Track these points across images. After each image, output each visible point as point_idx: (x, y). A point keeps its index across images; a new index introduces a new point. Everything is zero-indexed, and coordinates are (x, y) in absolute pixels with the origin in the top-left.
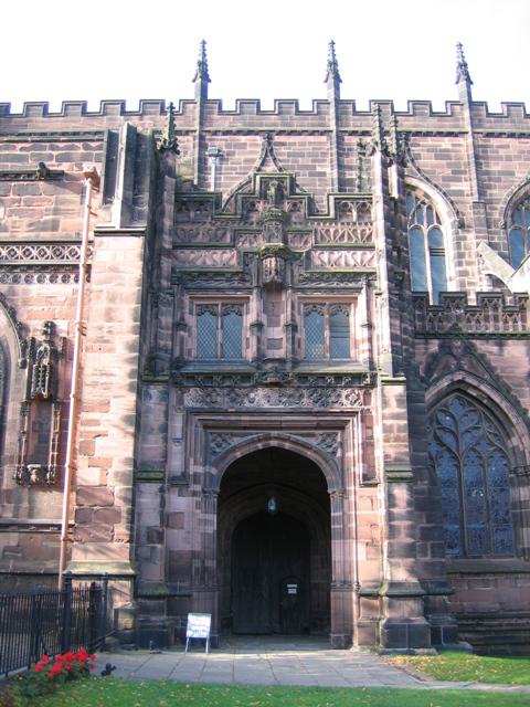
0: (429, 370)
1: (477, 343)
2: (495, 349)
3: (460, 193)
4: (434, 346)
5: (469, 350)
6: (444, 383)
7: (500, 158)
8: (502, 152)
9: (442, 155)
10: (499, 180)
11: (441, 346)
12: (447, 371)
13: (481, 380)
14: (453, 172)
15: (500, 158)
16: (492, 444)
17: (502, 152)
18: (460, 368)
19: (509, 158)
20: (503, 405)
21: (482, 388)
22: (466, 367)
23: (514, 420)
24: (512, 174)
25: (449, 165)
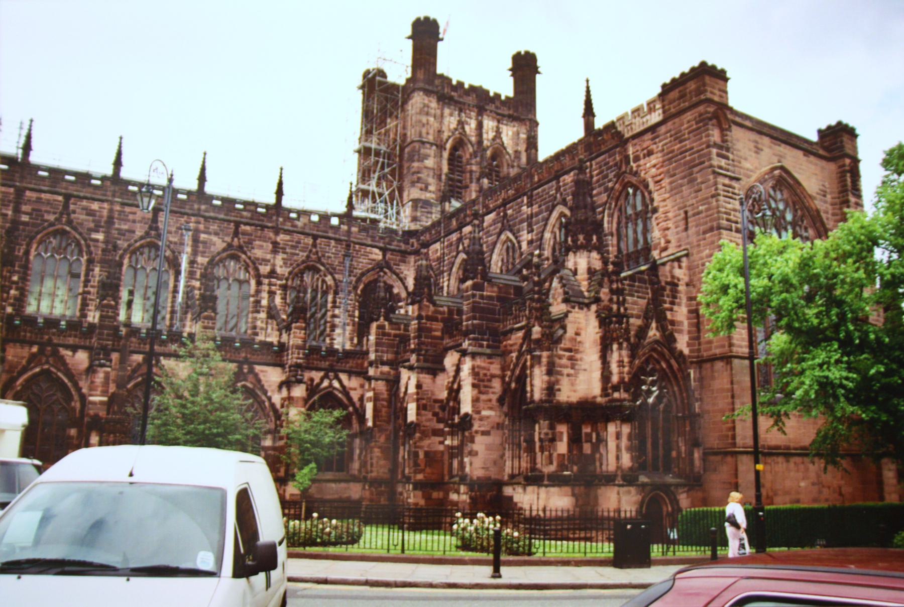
0: (29, 361)
1: (61, 349)
2: (70, 353)
3: (97, 241)
4: (35, 349)
5: (56, 354)
6: (37, 370)
7: (129, 221)
8: (131, 217)
9: (91, 213)
10: (124, 235)
11: (39, 350)
12: (39, 364)
13: (59, 370)
14: (96, 226)
15: (129, 221)
16: (61, 404)
17: (131, 217)
18: (47, 362)
19: (134, 221)
20: (69, 384)
21: (60, 374)
22: (51, 362)
23: (74, 393)
24: (134, 232)
25: (94, 221)
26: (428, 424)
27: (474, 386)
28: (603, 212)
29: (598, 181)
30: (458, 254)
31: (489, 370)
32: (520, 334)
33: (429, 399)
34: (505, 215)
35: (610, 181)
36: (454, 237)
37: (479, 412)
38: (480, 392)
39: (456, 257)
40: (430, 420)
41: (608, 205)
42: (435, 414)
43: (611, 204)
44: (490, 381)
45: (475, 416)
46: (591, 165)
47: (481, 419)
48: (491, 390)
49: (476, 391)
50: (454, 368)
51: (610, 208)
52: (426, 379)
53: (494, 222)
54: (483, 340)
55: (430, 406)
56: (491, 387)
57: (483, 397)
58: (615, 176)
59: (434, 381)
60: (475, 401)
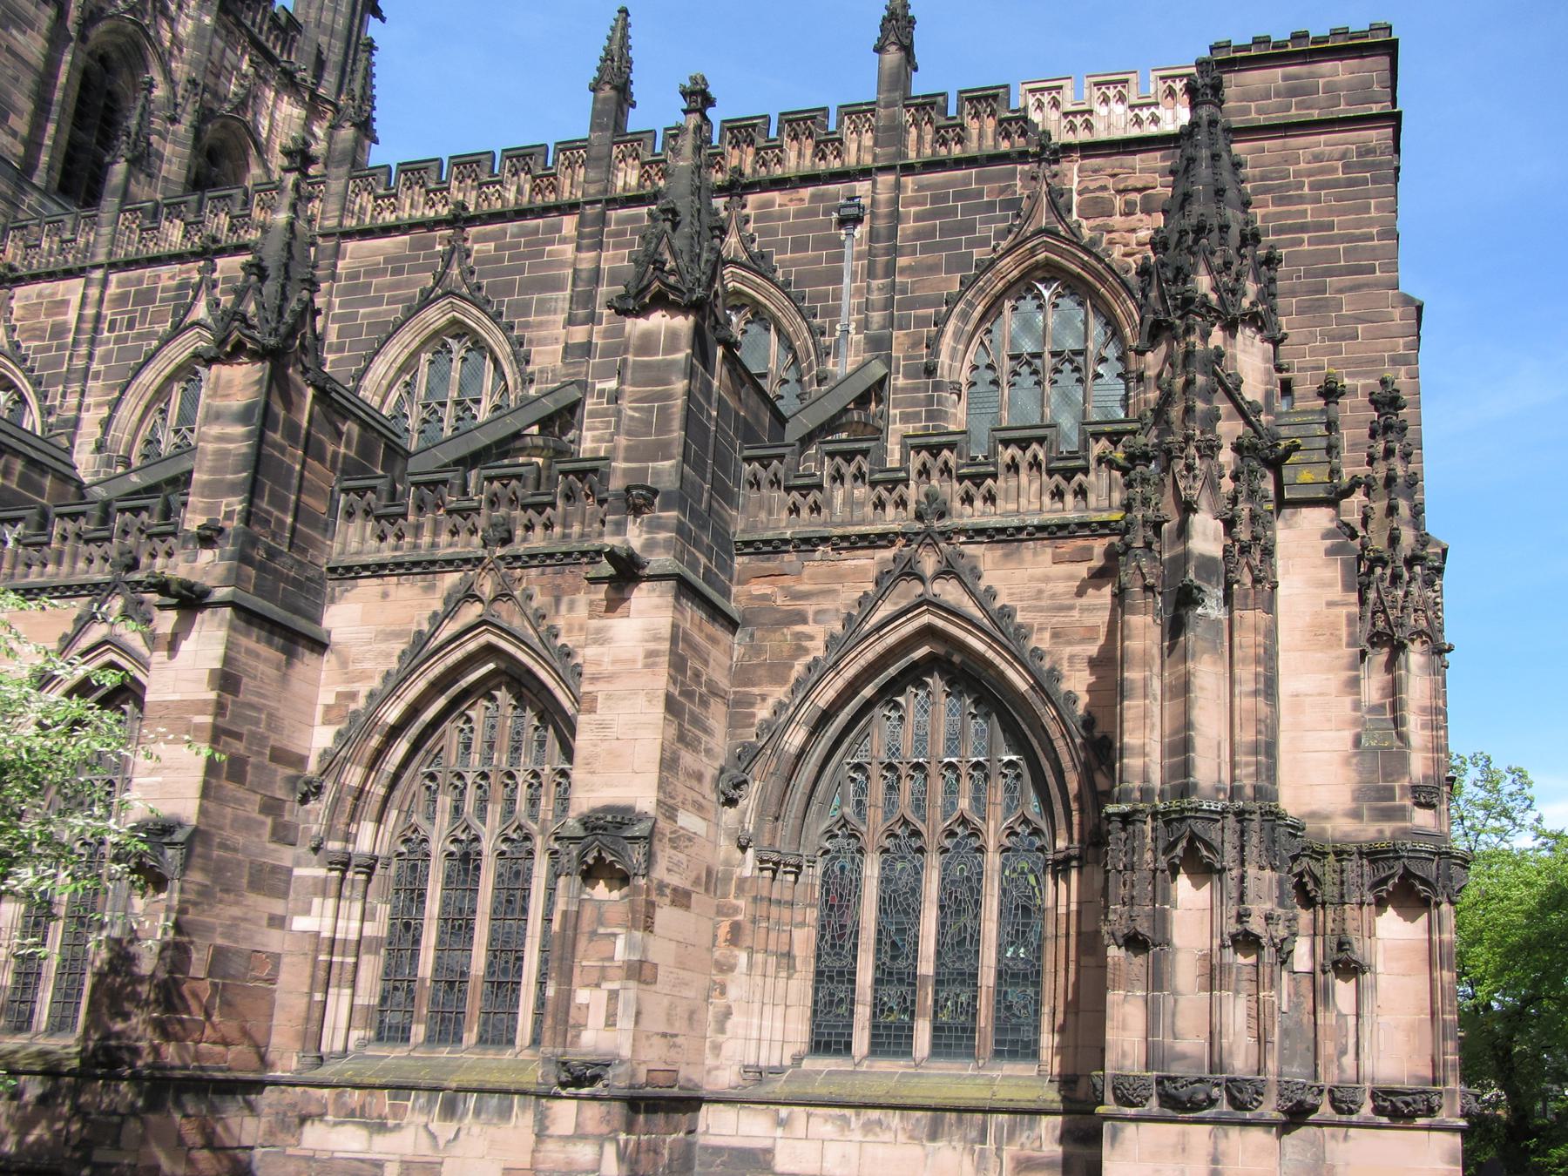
26: (240, 839)
27: (671, 705)
28: (940, 322)
29: (918, 235)
30: (178, 330)
31: (706, 663)
32: (869, 562)
33: (262, 740)
34: (456, 251)
35: (984, 242)
36: (168, 276)
37: (670, 812)
38: (681, 738)
39: (166, 341)
40: (248, 825)
41: (961, 306)
42: (272, 807)
43: (971, 305)
44: (704, 703)
45: (663, 824)
46: (898, 186)
47: (674, 843)
48: (704, 738)
49: (672, 731)
50: (399, 646)
51: (965, 317)
52: (261, 654)
53: (395, 265)
54: (697, 543)
55: (259, 768)
56: (706, 730)
57: (687, 759)
58: (1001, 235)
59: (284, 680)
60: (668, 764)
